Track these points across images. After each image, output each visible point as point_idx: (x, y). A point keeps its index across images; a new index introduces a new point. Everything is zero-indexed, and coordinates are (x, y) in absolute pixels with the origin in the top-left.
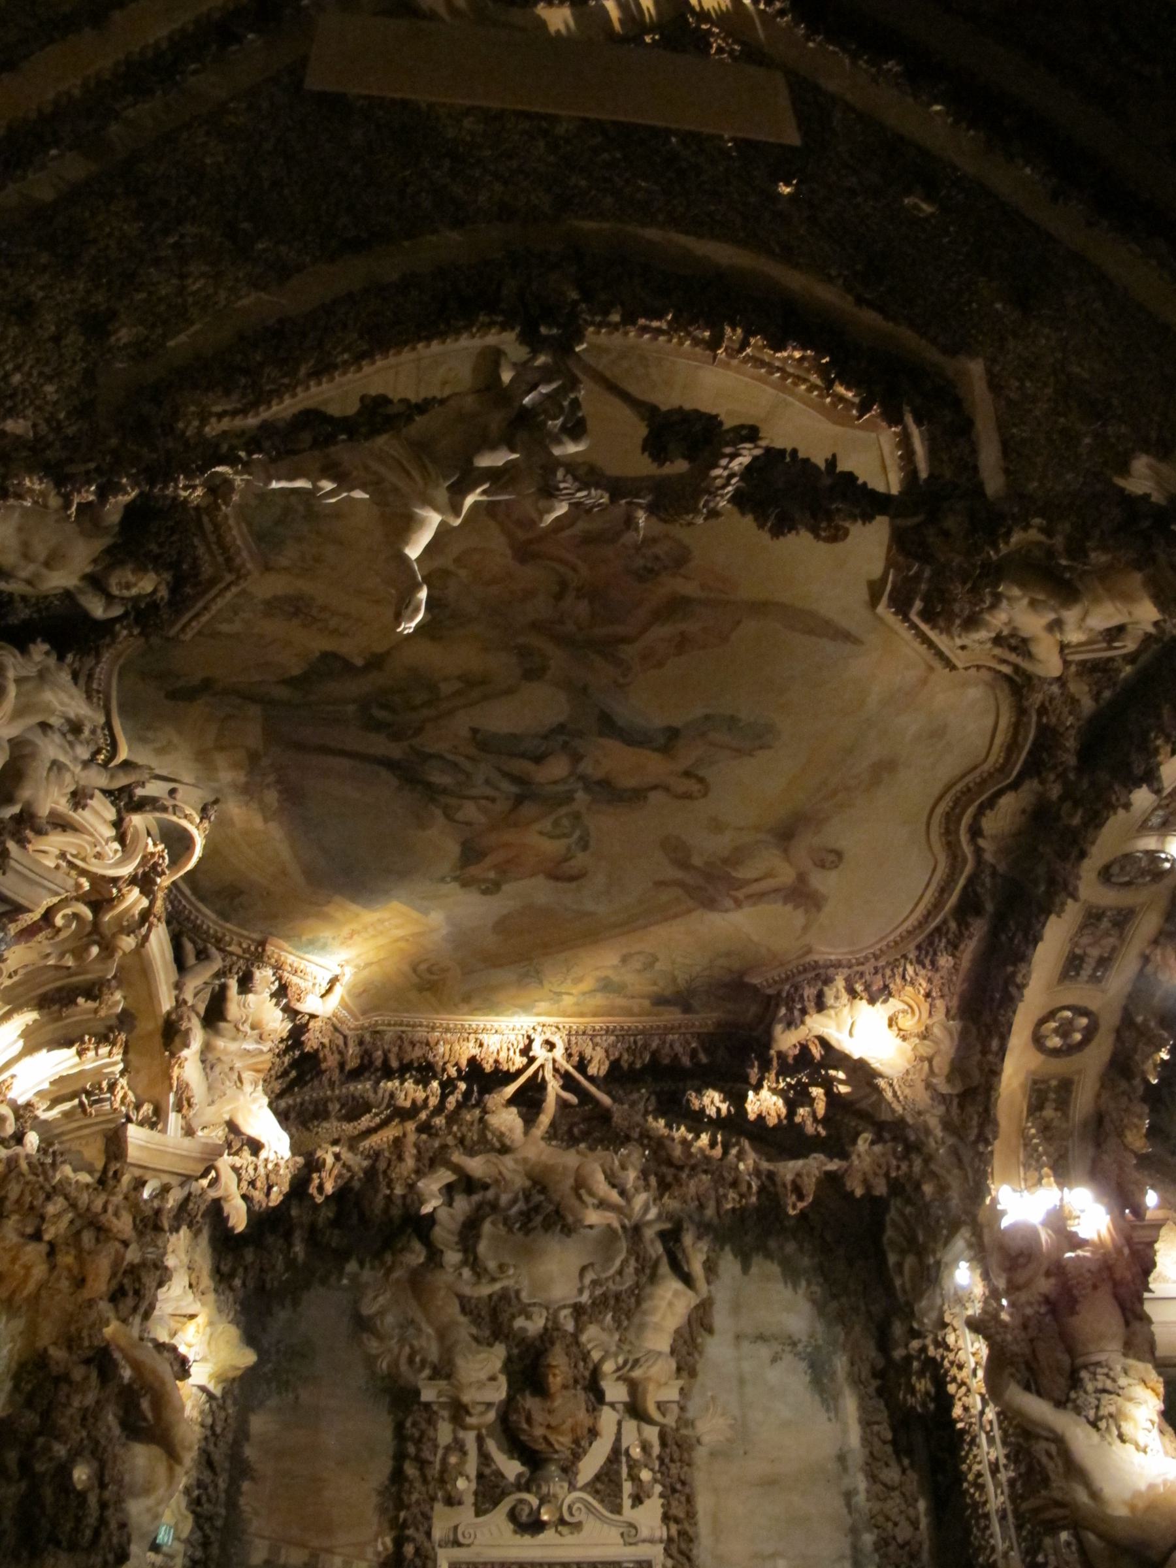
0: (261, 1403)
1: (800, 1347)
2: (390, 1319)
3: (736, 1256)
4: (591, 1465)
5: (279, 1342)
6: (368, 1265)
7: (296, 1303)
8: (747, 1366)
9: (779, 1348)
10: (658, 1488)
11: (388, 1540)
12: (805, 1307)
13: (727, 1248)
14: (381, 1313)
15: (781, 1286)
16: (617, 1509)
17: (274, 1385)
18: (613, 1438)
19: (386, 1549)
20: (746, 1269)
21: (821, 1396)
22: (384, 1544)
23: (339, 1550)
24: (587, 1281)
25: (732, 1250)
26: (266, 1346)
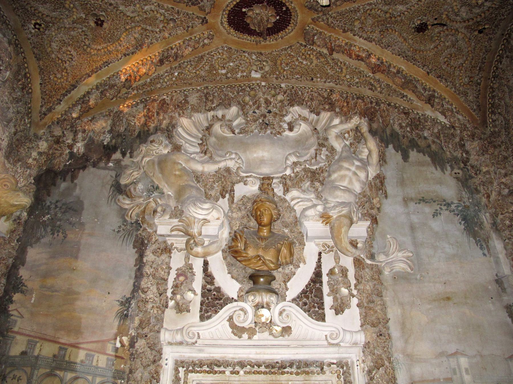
0: (38, 239)
1: (453, 207)
2: (140, 186)
3: (397, 152)
4: (298, 283)
5: (57, 202)
6: (128, 155)
7: (73, 178)
8: (415, 219)
9: (438, 207)
10: (355, 301)
11: (125, 339)
12: (452, 182)
13: (391, 146)
14: (134, 183)
15: (433, 169)
16: (321, 318)
17: (49, 229)
18: (314, 265)
19: (123, 345)
20: (405, 157)
21: (475, 238)
22: (121, 342)
23: (82, 346)
24: (289, 163)
25: (394, 147)
26: (48, 204)
